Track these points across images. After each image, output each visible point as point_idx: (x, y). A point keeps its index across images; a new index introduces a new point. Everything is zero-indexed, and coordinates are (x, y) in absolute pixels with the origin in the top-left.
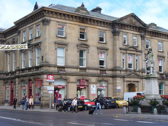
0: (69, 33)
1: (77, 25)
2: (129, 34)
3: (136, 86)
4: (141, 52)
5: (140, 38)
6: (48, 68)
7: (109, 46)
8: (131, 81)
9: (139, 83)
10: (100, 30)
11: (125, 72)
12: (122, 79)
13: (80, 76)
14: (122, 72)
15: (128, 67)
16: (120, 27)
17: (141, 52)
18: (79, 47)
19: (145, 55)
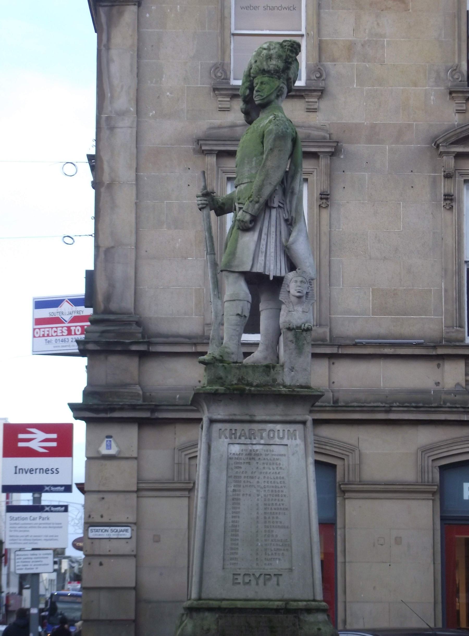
0: (350, 47)
6: (132, 364)
18: (458, 156)
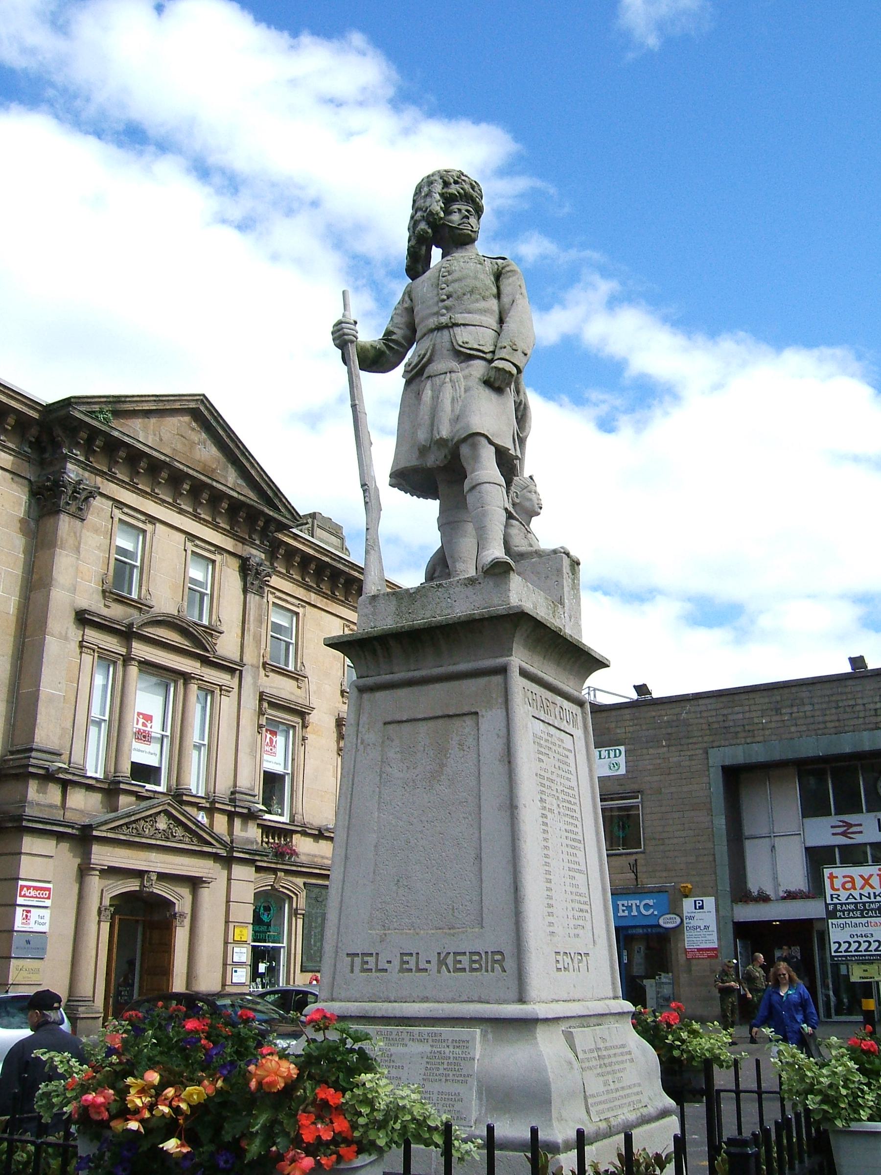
3: (182, 915)
4: (232, 669)
8: (140, 874)
9: (205, 893)
17: (231, 671)
19: (261, 700)
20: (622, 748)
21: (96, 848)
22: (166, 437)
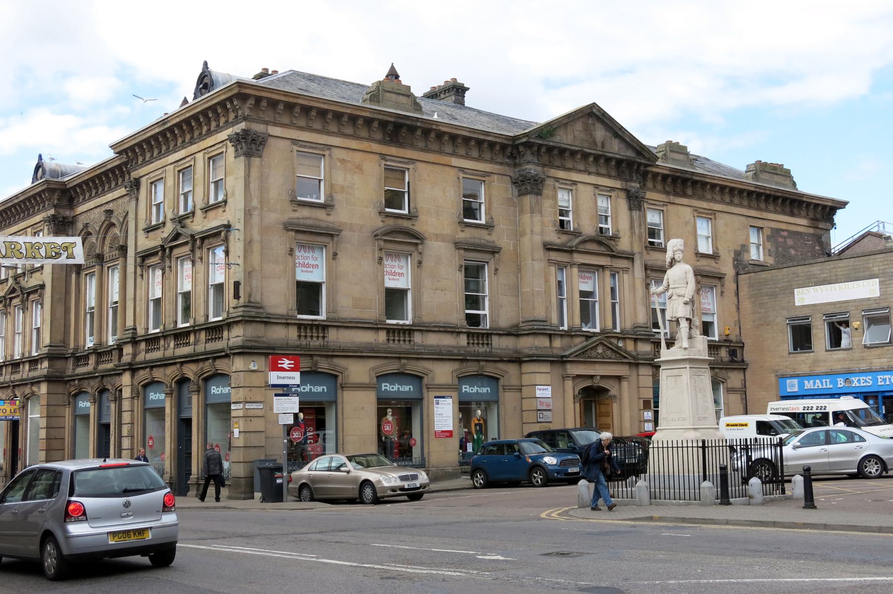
0: (342, 187)
1: (372, 156)
2: (580, 186)
3: (615, 396)
4: (630, 258)
5: (623, 204)
6: (261, 327)
7: (501, 238)
8: (592, 377)
9: (625, 384)
10: (465, 173)
11: (566, 340)
12: (558, 370)
13: (386, 361)
14: (557, 343)
15: (577, 321)
16: (545, 159)
18: (385, 241)
19: (646, 269)
20: (877, 280)
21: (568, 366)
22: (577, 133)
